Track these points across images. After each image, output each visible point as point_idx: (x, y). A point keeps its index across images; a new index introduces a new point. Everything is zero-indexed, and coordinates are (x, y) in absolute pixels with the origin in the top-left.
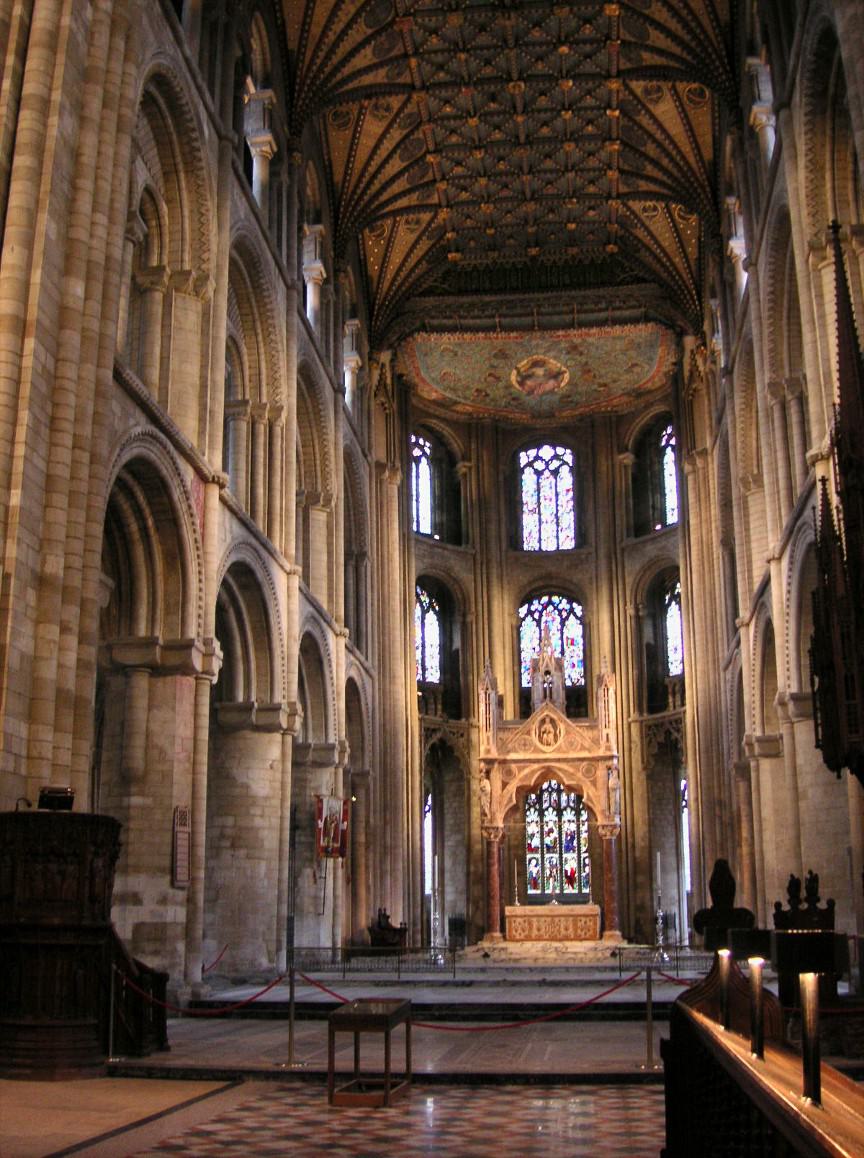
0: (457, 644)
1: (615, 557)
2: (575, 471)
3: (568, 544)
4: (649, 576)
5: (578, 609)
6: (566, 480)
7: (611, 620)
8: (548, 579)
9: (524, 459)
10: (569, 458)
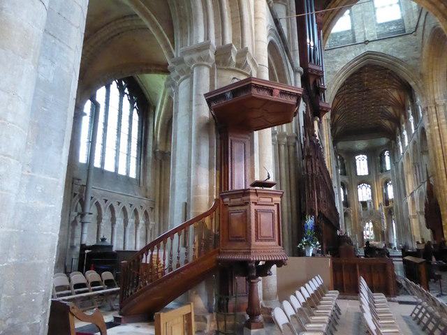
0: (347, 193)
1: (377, 177)
2: (368, 160)
3: (367, 173)
4: (384, 181)
5: (369, 186)
6: (366, 162)
7: (378, 188)
8: (363, 180)
9: (357, 157)
10: (365, 157)
